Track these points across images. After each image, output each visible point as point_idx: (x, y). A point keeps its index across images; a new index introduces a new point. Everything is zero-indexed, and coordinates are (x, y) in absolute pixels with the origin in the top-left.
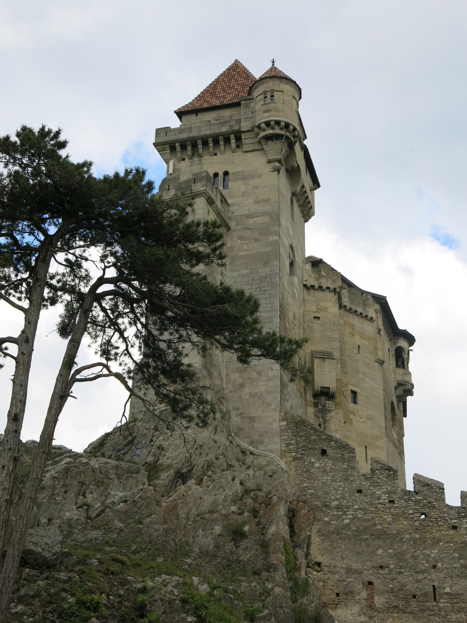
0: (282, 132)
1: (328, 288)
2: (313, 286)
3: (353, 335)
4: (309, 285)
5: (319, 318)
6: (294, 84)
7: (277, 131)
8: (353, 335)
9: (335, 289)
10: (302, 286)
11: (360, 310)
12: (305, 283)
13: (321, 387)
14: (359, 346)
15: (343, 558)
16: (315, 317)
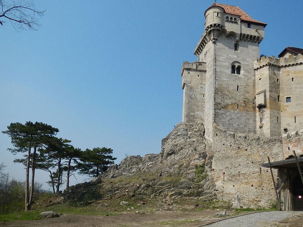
0: (212, 29)
1: (264, 66)
2: (258, 68)
3: (289, 75)
4: (256, 68)
5: (261, 79)
6: (214, 7)
7: (209, 30)
8: (289, 75)
9: (266, 64)
10: (254, 71)
11: (291, 63)
12: (255, 68)
13: (259, 105)
14: (293, 78)
15: (218, 167)
16: (260, 79)
